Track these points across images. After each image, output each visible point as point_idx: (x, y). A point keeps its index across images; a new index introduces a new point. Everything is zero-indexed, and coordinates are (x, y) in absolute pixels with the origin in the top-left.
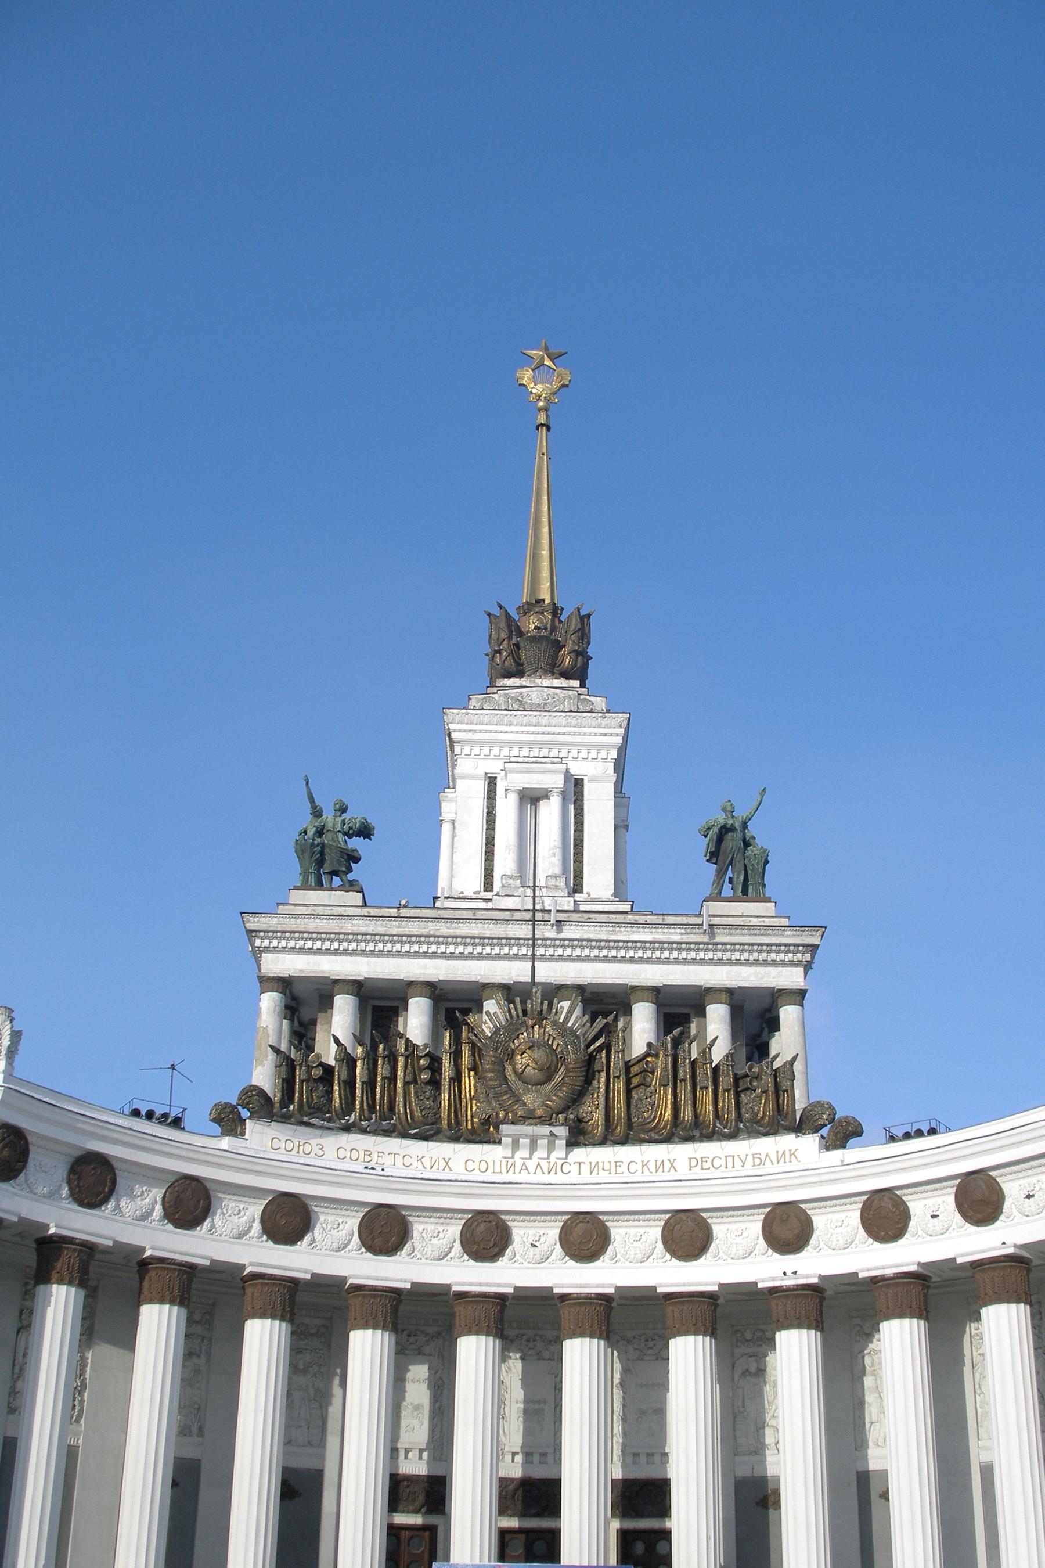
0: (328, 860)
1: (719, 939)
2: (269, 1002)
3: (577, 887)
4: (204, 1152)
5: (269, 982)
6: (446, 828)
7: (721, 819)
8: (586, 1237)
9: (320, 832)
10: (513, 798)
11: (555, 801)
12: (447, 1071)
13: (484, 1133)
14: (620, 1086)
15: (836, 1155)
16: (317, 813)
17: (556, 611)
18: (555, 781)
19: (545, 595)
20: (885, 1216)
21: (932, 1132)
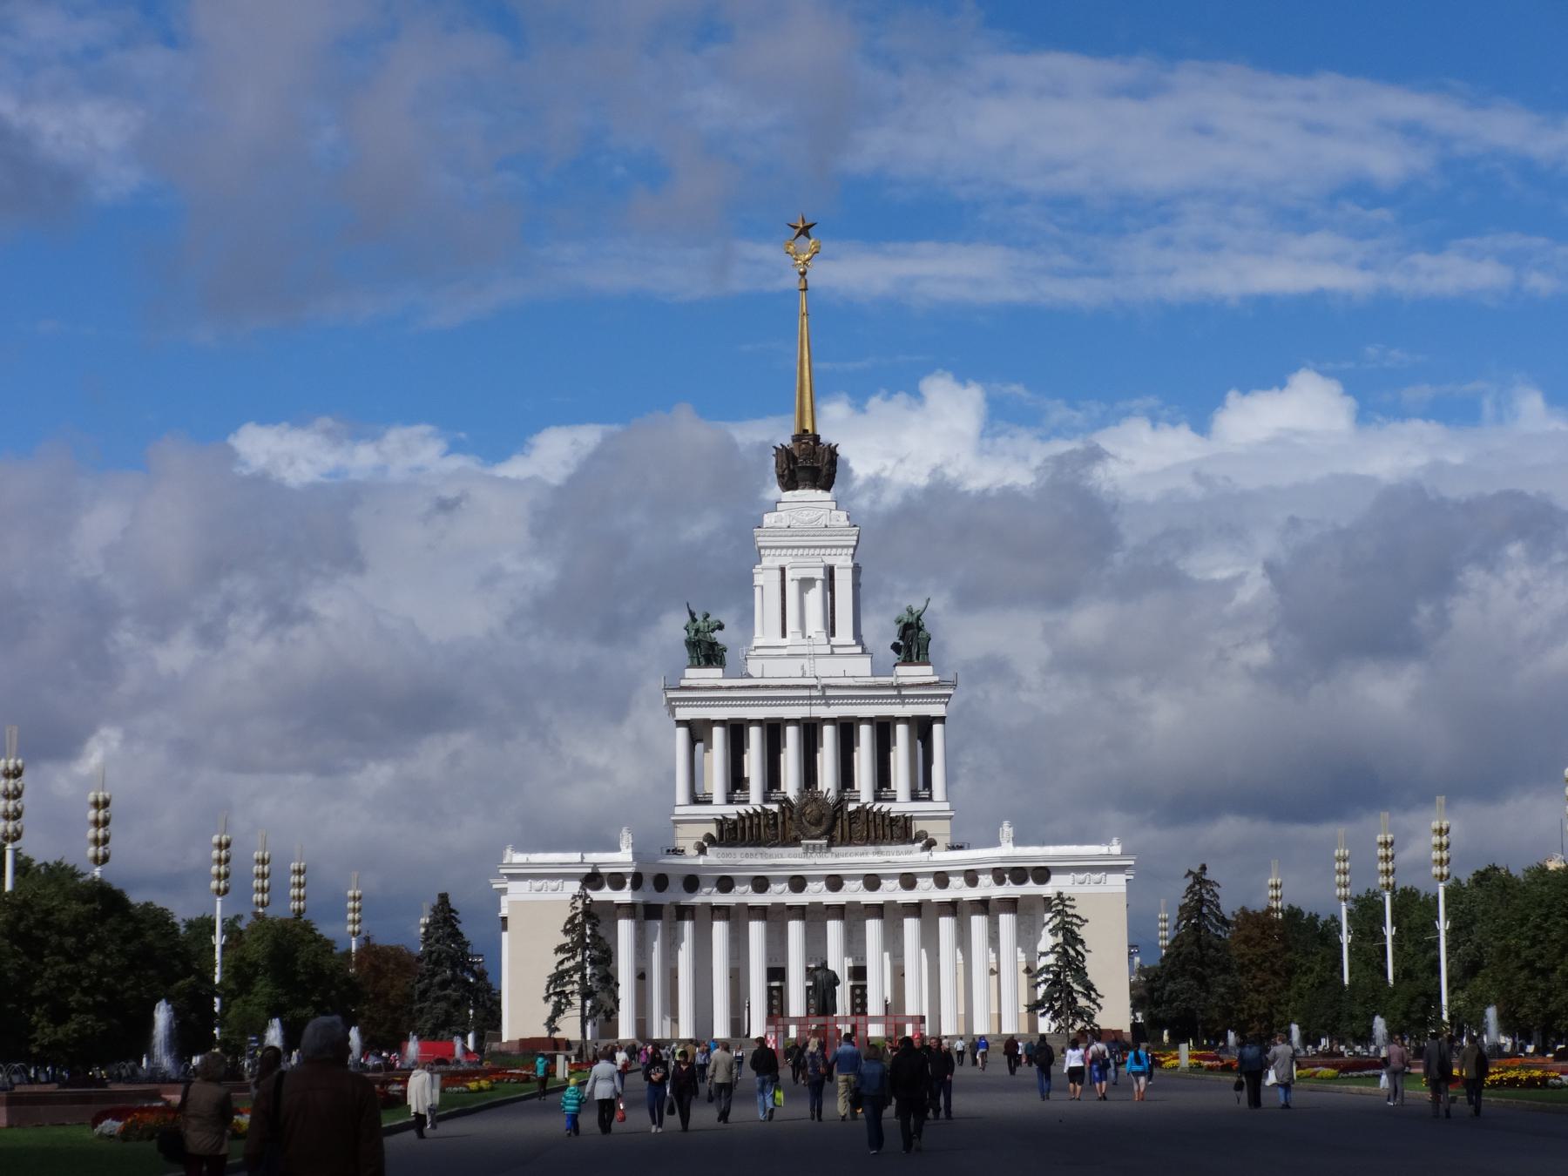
0: (706, 652)
1: (904, 692)
2: (682, 733)
3: (833, 633)
4: (692, 859)
5: (680, 723)
6: (757, 591)
7: (906, 618)
8: (835, 883)
9: (697, 631)
10: (795, 584)
11: (819, 584)
12: (780, 819)
13: (795, 842)
14: (846, 823)
15: (926, 854)
16: (692, 615)
17: (816, 438)
18: (819, 574)
19: (808, 427)
20: (942, 880)
21: (960, 848)
